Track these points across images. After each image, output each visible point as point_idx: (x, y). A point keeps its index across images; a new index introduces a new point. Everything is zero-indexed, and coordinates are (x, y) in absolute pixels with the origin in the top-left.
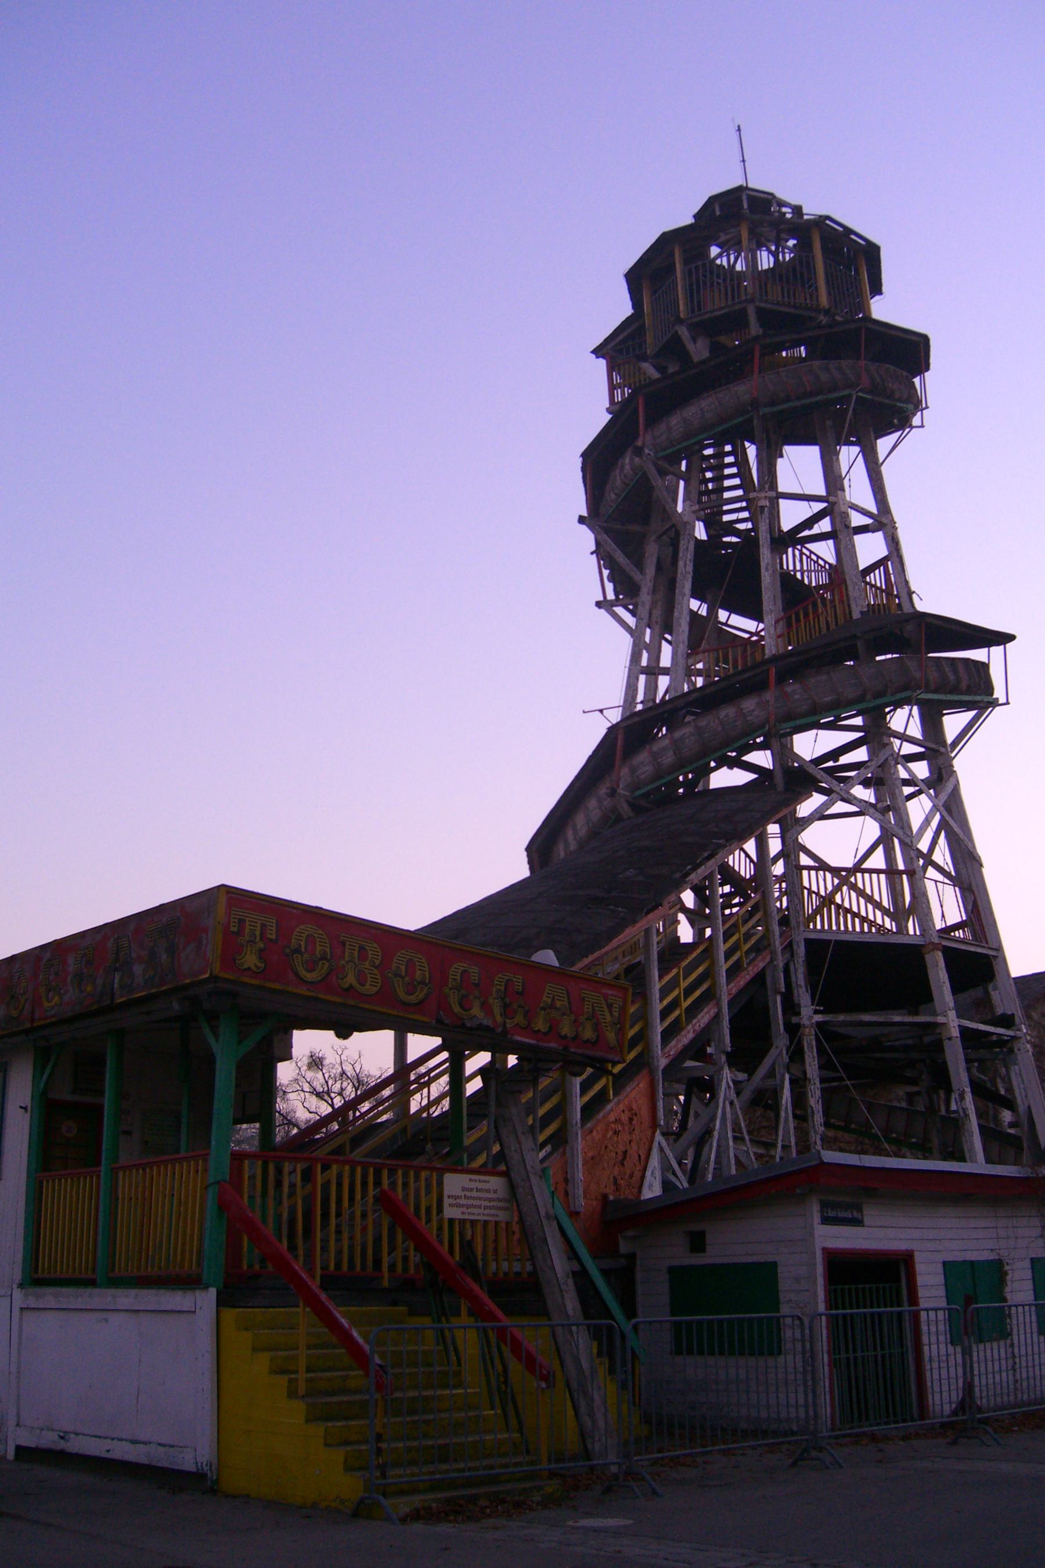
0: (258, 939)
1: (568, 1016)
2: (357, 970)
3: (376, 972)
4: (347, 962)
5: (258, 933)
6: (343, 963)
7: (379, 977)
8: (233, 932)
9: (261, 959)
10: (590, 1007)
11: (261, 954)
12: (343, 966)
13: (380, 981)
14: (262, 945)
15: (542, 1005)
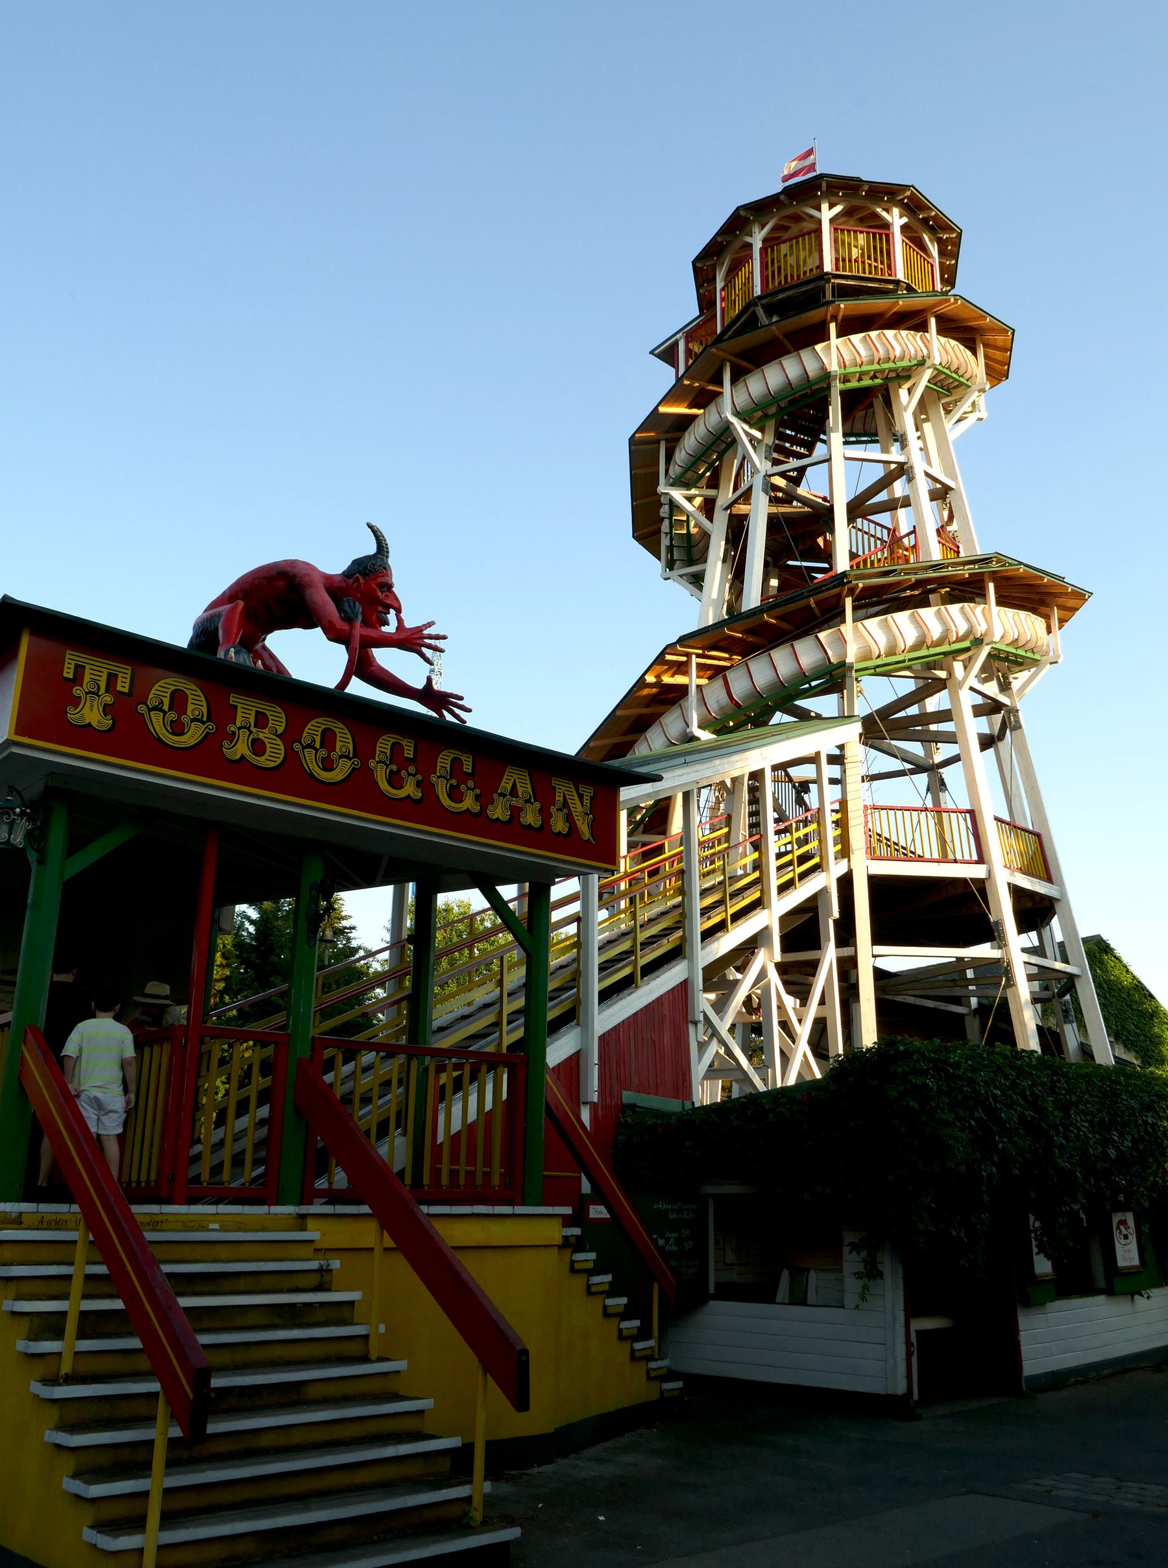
0: (102, 691)
1: (532, 804)
2: (250, 739)
3: (279, 742)
4: (239, 728)
5: (103, 685)
6: (232, 729)
7: (282, 747)
8: (68, 679)
9: (105, 714)
10: (562, 795)
11: (107, 710)
12: (234, 733)
13: (282, 752)
14: (109, 699)
15: (499, 791)
